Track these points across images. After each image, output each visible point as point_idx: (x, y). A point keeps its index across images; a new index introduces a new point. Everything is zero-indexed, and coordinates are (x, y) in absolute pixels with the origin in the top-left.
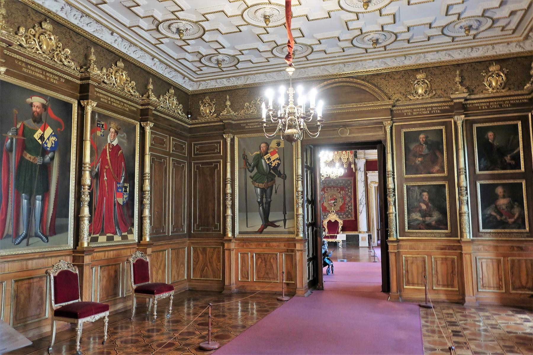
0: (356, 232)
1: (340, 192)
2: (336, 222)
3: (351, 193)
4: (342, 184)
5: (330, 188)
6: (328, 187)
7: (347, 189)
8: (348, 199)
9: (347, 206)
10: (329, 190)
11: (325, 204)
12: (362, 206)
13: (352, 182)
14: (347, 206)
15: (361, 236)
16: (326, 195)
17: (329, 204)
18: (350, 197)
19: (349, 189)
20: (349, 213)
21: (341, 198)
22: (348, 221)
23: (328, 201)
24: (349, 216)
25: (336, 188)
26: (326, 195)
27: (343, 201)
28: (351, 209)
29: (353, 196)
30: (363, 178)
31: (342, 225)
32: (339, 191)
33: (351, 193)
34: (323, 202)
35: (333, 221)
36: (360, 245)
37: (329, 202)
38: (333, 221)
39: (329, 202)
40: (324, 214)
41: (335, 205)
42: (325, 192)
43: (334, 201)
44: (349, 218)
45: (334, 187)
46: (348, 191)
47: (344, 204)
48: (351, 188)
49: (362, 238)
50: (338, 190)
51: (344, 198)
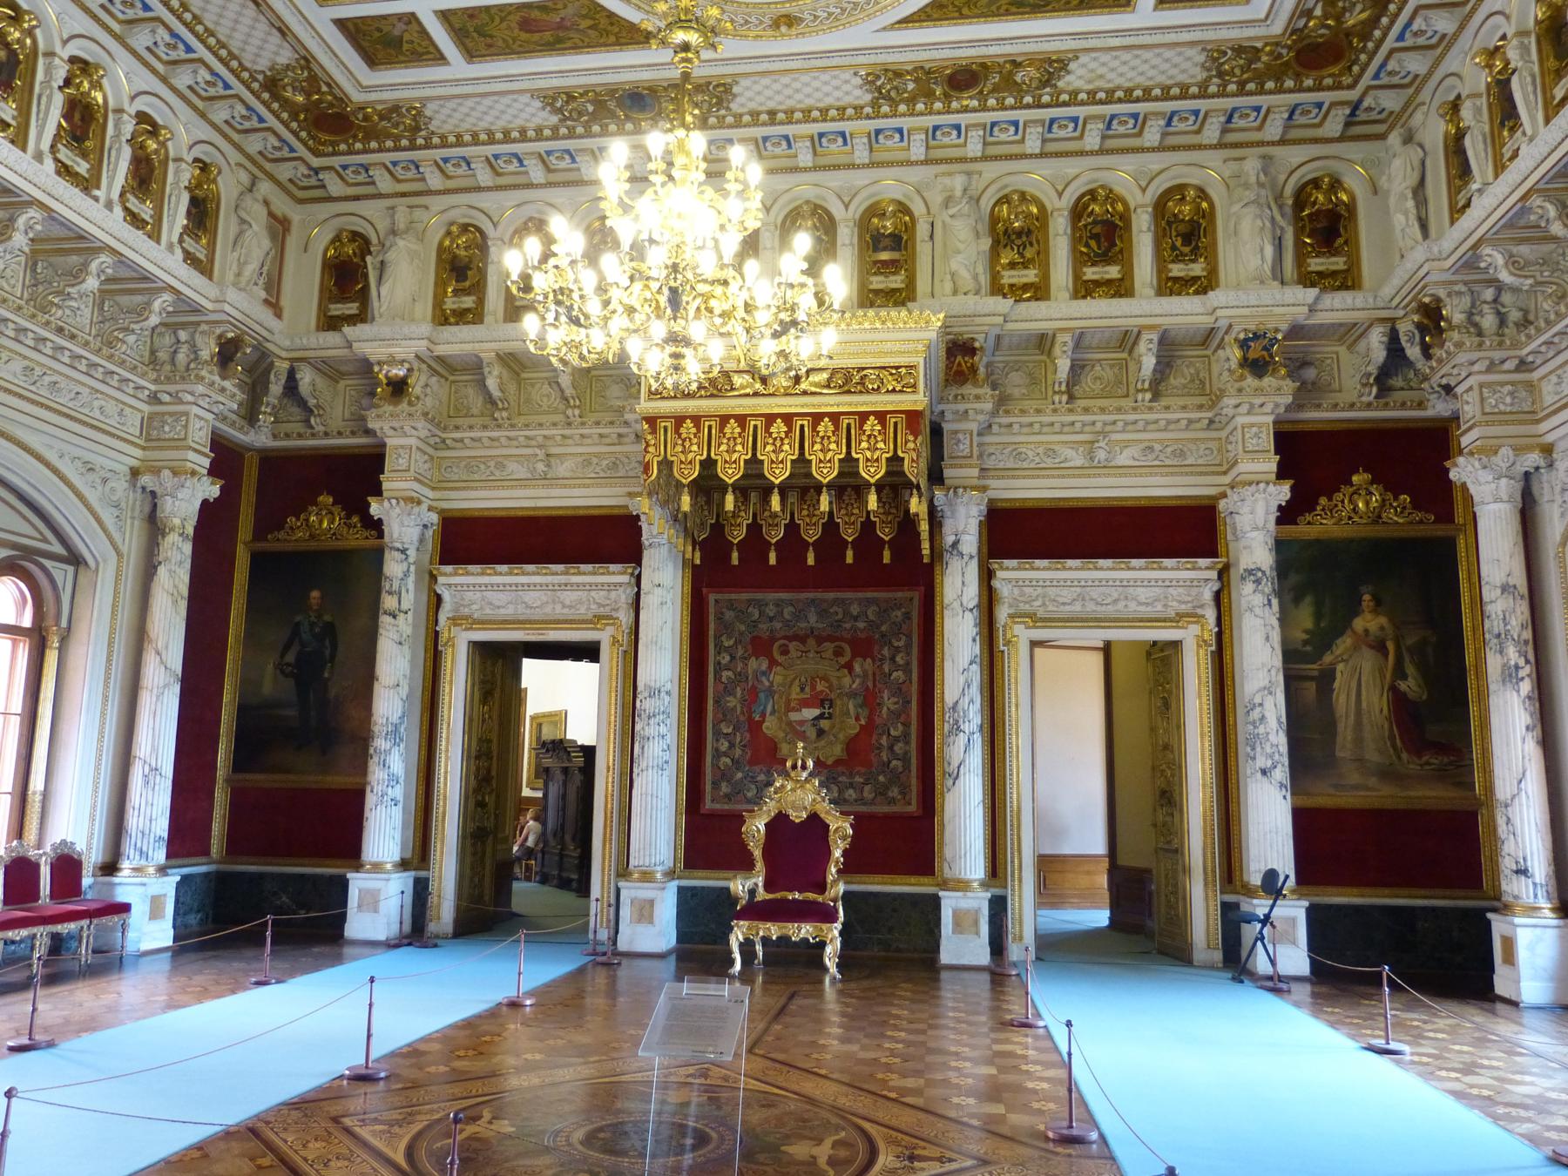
0: (925, 880)
1: (849, 667)
2: (816, 824)
3: (906, 669)
5: (802, 639)
7: (886, 652)
8: (889, 702)
9: (884, 741)
10: (794, 653)
11: (770, 726)
12: (962, 739)
14: (884, 741)
15: (950, 904)
16: (778, 679)
17: (790, 723)
18: (899, 691)
19: (897, 649)
20: (896, 778)
21: (853, 695)
22: (888, 817)
23: (789, 709)
24: (894, 792)
25: (829, 647)
26: (778, 679)
27: (864, 713)
28: (905, 759)
29: (915, 688)
30: (972, 593)
32: (843, 660)
33: (907, 671)
34: (763, 715)
35: (798, 816)
36: (946, 957)
37: (794, 716)
38: (798, 816)
39: (794, 716)
42: (773, 663)
43: (816, 712)
44: (892, 801)
45: (820, 640)
46: (893, 659)
47: (868, 729)
48: (908, 645)
49: (957, 914)
50: (838, 653)
51: (869, 699)
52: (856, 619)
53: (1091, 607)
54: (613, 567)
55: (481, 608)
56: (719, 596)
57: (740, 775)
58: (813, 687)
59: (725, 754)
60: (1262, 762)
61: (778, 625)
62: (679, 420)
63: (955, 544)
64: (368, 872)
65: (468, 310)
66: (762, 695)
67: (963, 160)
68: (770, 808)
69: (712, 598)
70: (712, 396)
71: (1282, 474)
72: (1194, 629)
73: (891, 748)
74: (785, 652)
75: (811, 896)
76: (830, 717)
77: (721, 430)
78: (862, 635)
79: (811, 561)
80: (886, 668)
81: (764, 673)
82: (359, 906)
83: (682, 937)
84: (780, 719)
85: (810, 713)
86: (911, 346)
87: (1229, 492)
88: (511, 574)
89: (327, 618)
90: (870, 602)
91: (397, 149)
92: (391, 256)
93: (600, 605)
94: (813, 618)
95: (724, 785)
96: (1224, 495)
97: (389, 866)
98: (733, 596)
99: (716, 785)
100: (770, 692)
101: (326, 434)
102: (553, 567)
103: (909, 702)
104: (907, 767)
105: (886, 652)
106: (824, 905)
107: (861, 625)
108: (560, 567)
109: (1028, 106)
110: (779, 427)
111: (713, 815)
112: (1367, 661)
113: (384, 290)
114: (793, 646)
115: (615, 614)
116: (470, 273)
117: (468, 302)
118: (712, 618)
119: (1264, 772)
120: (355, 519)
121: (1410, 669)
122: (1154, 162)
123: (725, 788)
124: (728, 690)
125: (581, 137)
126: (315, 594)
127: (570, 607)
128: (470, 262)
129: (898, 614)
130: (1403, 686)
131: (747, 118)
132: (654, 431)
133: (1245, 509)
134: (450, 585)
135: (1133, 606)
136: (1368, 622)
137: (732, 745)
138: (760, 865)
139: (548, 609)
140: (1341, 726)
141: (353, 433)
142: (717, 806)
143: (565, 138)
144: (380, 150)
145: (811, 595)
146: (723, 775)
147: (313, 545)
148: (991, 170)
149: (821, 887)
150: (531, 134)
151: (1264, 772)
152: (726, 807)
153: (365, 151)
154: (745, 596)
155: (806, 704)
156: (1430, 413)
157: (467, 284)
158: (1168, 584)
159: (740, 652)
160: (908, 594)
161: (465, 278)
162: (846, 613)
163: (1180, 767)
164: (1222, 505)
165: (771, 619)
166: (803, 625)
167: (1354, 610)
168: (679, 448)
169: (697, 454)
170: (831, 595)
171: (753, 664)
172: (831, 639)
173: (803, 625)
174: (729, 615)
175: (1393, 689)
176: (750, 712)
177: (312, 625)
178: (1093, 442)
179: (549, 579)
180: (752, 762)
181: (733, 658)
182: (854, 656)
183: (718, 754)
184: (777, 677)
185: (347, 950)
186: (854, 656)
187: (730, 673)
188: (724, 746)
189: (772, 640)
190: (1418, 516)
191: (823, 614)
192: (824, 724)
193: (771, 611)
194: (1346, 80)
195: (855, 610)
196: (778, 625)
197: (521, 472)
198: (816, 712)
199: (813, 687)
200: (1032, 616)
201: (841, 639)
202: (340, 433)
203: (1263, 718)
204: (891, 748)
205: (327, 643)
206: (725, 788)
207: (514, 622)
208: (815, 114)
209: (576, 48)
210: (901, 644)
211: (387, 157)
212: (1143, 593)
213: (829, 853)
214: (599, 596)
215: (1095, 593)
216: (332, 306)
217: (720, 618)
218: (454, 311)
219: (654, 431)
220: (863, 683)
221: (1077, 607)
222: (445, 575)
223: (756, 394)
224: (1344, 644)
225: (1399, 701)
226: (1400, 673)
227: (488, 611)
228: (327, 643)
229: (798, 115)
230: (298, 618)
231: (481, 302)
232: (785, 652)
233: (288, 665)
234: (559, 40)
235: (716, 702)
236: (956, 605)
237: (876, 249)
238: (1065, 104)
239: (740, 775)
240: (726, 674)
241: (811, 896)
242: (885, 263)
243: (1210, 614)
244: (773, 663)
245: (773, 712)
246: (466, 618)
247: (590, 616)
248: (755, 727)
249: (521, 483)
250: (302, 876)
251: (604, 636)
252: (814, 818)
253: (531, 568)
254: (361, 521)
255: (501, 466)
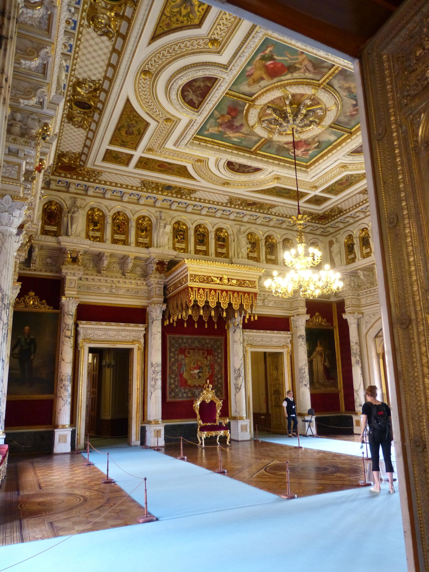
1: (206, 358)
2: (212, 403)
4: (209, 346)
5: (193, 349)
6: (191, 349)
7: (216, 354)
8: (217, 368)
9: (216, 379)
11: (185, 375)
12: (241, 378)
13: (223, 343)
14: (216, 379)
16: (187, 361)
17: (191, 374)
18: (219, 365)
21: (207, 366)
25: (201, 352)
27: (211, 371)
31: (220, 408)
32: (205, 356)
33: (221, 359)
34: (183, 372)
38: (208, 401)
40: (183, 391)
41: (199, 377)
42: (186, 356)
43: (198, 371)
45: (199, 350)
48: (221, 352)
50: (203, 354)
51: (212, 367)
52: (208, 344)
53: (264, 343)
54: (140, 325)
55: (93, 336)
56: (170, 336)
57: (177, 390)
58: (197, 364)
59: (173, 384)
60: (305, 383)
61: (187, 345)
62: (199, 289)
63: (238, 325)
64: (60, 428)
65: (98, 237)
66: (183, 366)
67: (242, 221)
68: (201, 399)
69: (168, 336)
70: (207, 283)
71: (308, 313)
72: (286, 349)
73: (218, 381)
74: (189, 353)
75: (213, 424)
76: (202, 372)
77: (210, 292)
78: (209, 348)
79: (196, 326)
80: (216, 358)
81: (184, 360)
82: (59, 441)
83: (166, 440)
84: (188, 373)
85: (196, 371)
86: (255, 276)
87: (295, 316)
88: (106, 325)
89: (32, 337)
90: (212, 339)
91: (83, 180)
92: (76, 215)
93: (134, 337)
94: (196, 343)
95: (173, 393)
96: (294, 316)
97: (67, 426)
98: (174, 336)
99: (170, 393)
100: (185, 365)
101: (35, 270)
102: (121, 324)
103: (222, 368)
104: (222, 387)
105: (216, 354)
106: (217, 425)
107: (209, 346)
108: (124, 324)
109: (261, 213)
110: (224, 293)
111: (170, 403)
112: (319, 358)
113: (74, 226)
114: (191, 351)
115: (139, 340)
116: (98, 225)
117: (98, 234)
118: (168, 342)
119: (305, 385)
120: (44, 301)
121: (327, 360)
122: (283, 232)
123: (173, 394)
124: (173, 364)
125: (145, 192)
126: (27, 328)
127: (124, 337)
128: (99, 221)
129: (219, 343)
130: (326, 364)
131: (193, 199)
132: (192, 291)
133: (300, 320)
134: (83, 328)
135: (273, 343)
136: (319, 349)
137: (175, 381)
138: (199, 416)
139: (117, 337)
140: (314, 373)
141: (46, 271)
142: (171, 400)
143: (140, 191)
144: (77, 179)
145: (196, 337)
146: (172, 390)
147: (27, 309)
148: (248, 226)
149: (215, 421)
150: (129, 187)
151: (305, 385)
152: (173, 400)
153: (71, 178)
154: (177, 336)
155: (195, 368)
156: (330, 300)
157: (96, 228)
158: (280, 338)
159: (176, 353)
160: (222, 337)
161: (97, 226)
162: (205, 342)
163: (283, 384)
164: (292, 318)
165: (185, 343)
166: (194, 345)
167: (316, 346)
168: (199, 297)
169: (204, 299)
170: (201, 337)
171: (180, 356)
172: (201, 349)
173: (194, 345)
174: (173, 341)
175: (324, 365)
176: (180, 371)
177: (26, 339)
178: (264, 300)
179: (119, 328)
180: (181, 386)
181: (174, 355)
182: (208, 354)
183: (171, 384)
184: (187, 361)
185: (55, 457)
186: (208, 354)
187: (174, 359)
188: (172, 381)
189: (185, 349)
190: (328, 324)
191: (199, 342)
192: (200, 374)
193: (185, 340)
194: (324, 223)
195: (208, 341)
196: (187, 345)
197: (107, 291)
198: (198, 371)
199: (197, 364)
200: (251, 345)
201: (204, 350)
202: (40, 271)
203: (305, 372)
204: (218, 381)
205: (32, 346)
206: (173, 394)
207: (105, 341)
208: (211, 202)
209: (168, 173)
210: (220, 351)
211: (77, 182)
212: (275, 340)
213: (216, 411)
214: (133, 334)
215: (265, 339)
216: (46, 226)
217: (170, 342)
218: (92, 237)
219: (192, 291)
220: (210, 363)
221: (261, 343)
222: (82, 324)
223: (218, 284)
224: (315, 353)
225: (325, 367)
226: (325, 361)
227: (96, 337)
228: (32, 346)
229: (207, 201)
230: (19, 337)
231: (103, 235)
232: (189, 353)
233: (15, 354)
234: (165, 171)
235: (170, 368)
236: (239, 341)
237: (219, 241)
238: (269, 214)
239: (177, 390)
240: (173, 360)
241: (213, 424)
242: (221, 245)
243: (290, 346)
244: (186, 356)
245: (186, 371)
246: (88, 339)
247: (131, 340)
248: (181, 375)
249: (107, 295)
250: (23, 433)
251: (135, 347)
252: (212, 402)
253: (114, 324)
254: (46, 302)
255: (99, 288)
